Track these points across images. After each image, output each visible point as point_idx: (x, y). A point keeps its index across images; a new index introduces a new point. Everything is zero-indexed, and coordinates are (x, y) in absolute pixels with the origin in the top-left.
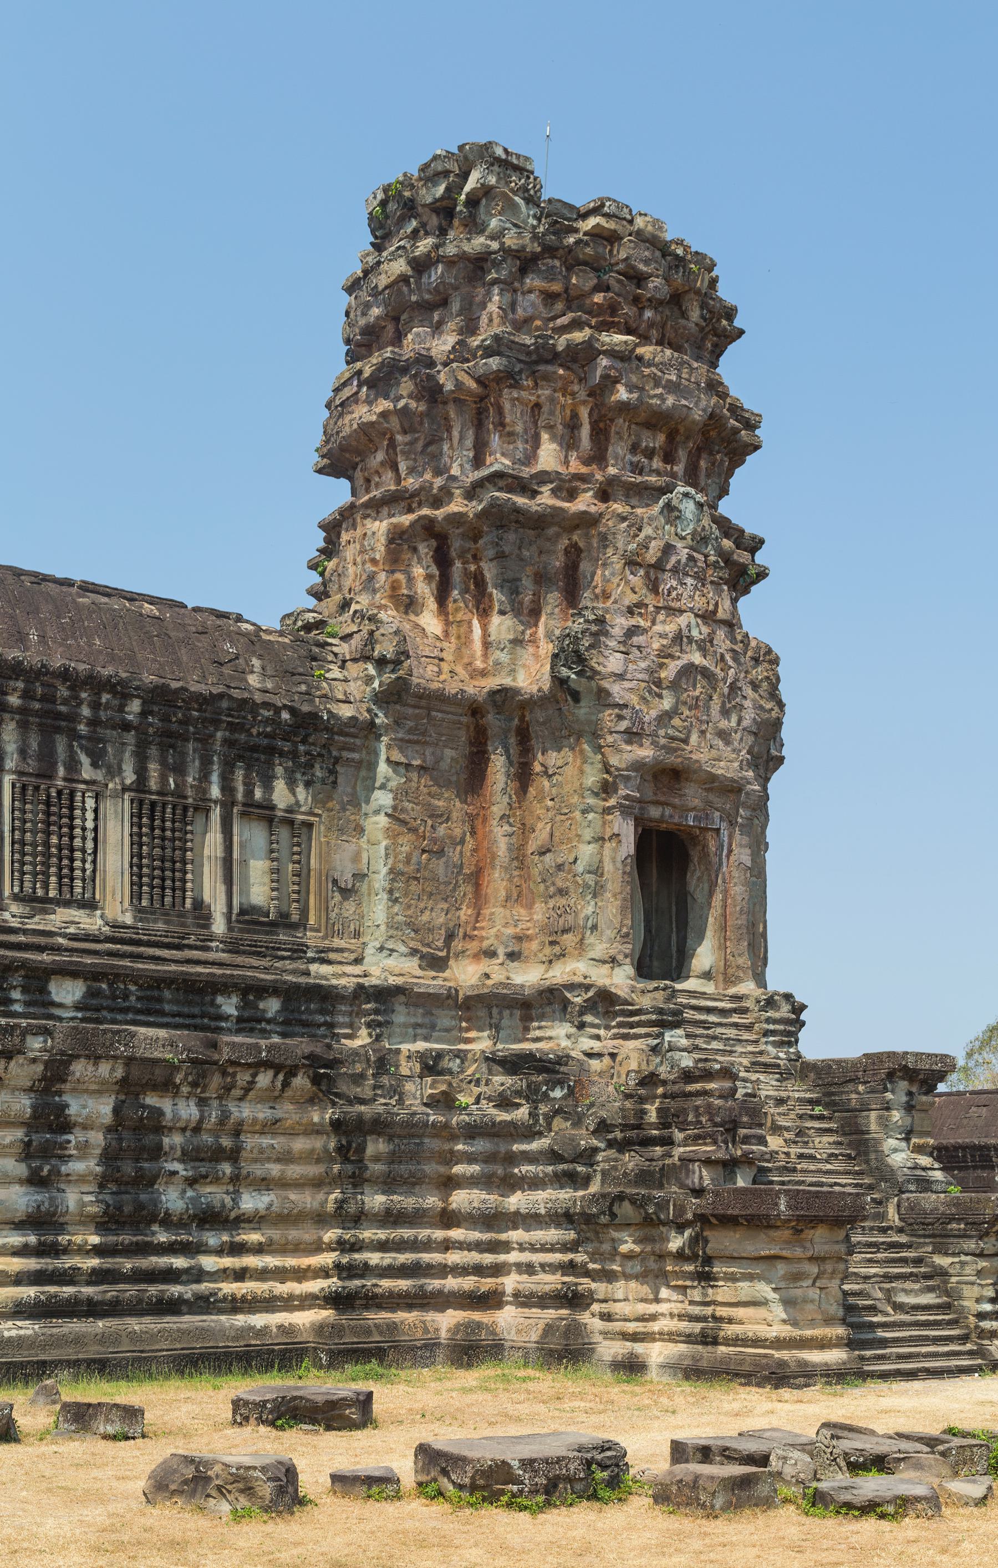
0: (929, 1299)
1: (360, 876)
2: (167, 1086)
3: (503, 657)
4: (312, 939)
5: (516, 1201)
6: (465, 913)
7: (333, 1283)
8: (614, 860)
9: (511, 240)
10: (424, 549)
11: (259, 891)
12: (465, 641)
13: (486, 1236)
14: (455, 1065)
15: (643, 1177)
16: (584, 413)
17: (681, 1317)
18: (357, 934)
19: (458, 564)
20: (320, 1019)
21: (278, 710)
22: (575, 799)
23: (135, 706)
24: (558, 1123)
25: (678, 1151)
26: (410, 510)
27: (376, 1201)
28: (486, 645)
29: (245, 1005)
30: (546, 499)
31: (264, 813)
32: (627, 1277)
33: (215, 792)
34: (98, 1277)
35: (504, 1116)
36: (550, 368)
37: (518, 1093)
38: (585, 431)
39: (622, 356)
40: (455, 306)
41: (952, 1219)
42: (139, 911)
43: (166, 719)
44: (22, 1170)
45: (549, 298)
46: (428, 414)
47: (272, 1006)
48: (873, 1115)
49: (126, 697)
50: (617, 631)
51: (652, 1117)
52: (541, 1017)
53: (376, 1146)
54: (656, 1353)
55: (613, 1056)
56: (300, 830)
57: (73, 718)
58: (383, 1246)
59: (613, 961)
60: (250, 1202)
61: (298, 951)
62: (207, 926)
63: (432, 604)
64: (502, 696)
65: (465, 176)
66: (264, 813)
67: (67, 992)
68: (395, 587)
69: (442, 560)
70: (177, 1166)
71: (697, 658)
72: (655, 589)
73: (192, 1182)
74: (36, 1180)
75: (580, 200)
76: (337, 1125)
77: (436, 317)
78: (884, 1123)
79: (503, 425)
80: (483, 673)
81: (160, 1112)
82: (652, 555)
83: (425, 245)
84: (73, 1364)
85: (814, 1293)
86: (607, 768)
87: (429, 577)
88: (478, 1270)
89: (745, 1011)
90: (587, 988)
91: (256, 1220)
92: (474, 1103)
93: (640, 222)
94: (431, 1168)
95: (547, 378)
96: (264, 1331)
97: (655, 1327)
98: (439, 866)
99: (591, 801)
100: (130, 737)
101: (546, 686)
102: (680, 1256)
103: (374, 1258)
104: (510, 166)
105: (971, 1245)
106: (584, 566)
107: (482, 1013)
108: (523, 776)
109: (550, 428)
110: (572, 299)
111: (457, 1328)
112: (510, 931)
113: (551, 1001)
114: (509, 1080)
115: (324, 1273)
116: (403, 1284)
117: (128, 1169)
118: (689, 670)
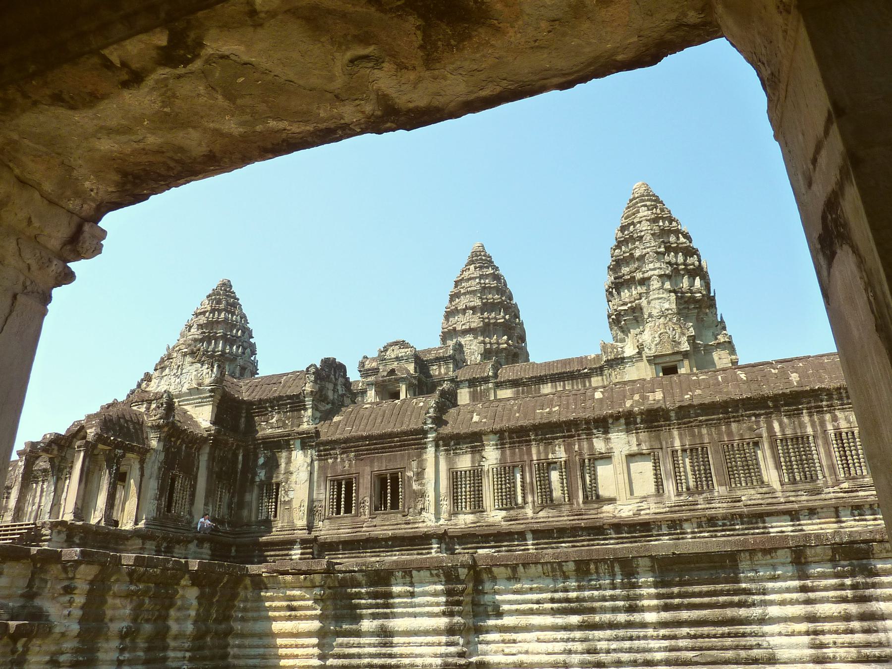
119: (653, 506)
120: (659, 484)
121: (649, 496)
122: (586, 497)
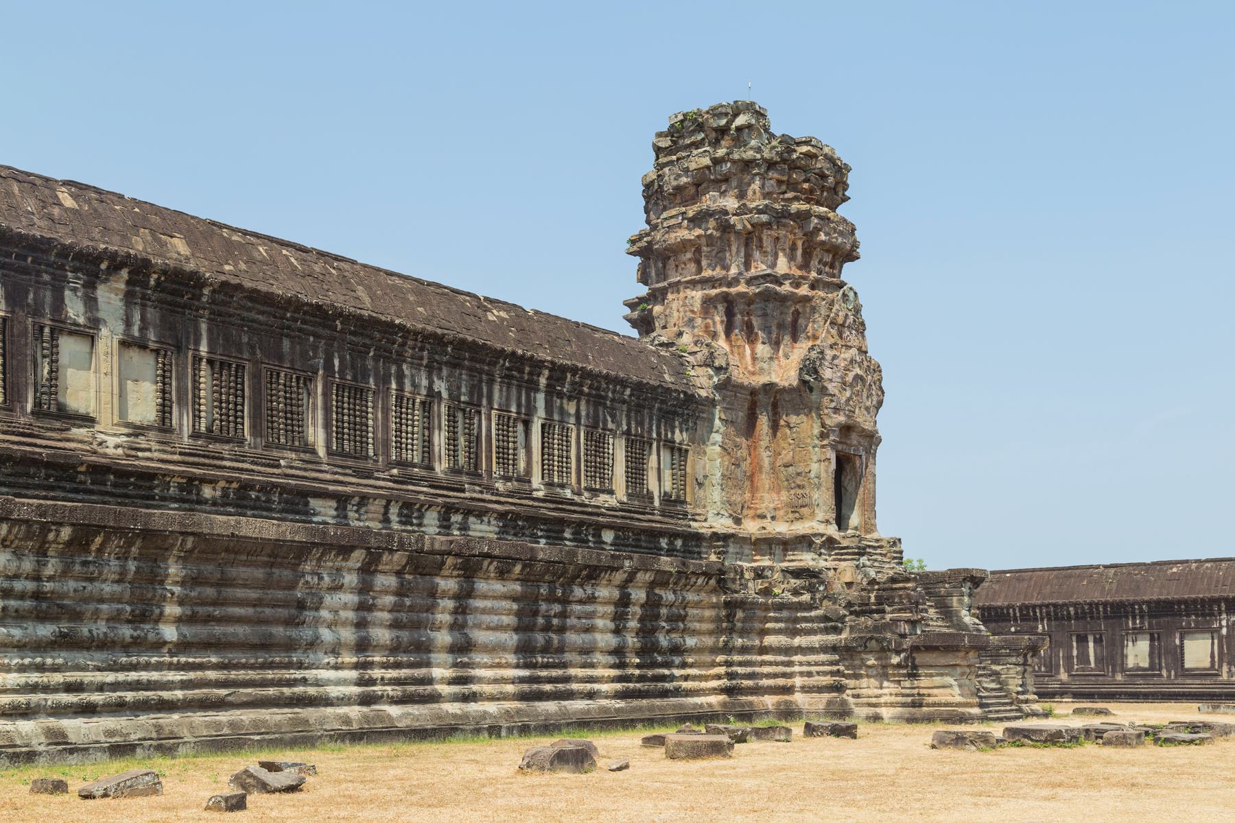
0: (993, 685)
1: (705, 477)
2: (664, 585)
3: (765, 366)
4: (689, 508)
5: (798, 641)
6: (748, 495)
7: (724, 682)
8: (827, 471)
9: (767, 154)
10: (721, 308)
11: (668, 486)
12: (742, 356)
13: (786, 659)
14: (769, 573)
15: (876, 629)
16: (800, 243)
17: (896, 695)
18: (704, 507)
19: (739, 316)
20: (696, 550)
21: (679, 393)
22: (809, 441)
23: (628, 392)
24: (825, 602)
25: (888, 617)
26: (714, 287)
27: (739, 642)
28: (754, 359)
29: (671, 543)
30: (786, 288)
31: (671, 446)
32: (868, 676)
33: (654, 436)
34: (641, 679)
35: (795, 599)
36: (787, 221)
37: (803, 588)
38: (799, 252)
39: (823, 218)
40: (734, 184)
41: (1003, 648)
42: (629, 495)
43: (638, 398)
44: (611, 625)
45: (780, 182)
46: (720, 238)
47: (679, 543)
48: (955, 599)
49: (625, 387)
50: (828, 358)
51: (873, 600)
53: (740, 614)
54: (885, 712)
55: (835, 569)
56: (683, 453)
57: (605, 398)
58: (741, 664)
59: (827, 521)
60: (691, 642)
61: (685, 514)
62: (652, 503)
63: (723, 336)
64: (769, 387)
65: (736, 115)
66: (671, 446)
67: (608, 536)
68: (707, 326)
69: (730, 314)
70: (664, 624)
71: (858, 371)
72: (841, 337)
73: (668, 632)
74: (617, 632)
75: (797, 135)
76: (727, 604)
77: (723, 188)
78: (961, 602)
79: (761, 247)
80: (753, 374)
81: (661, 597)
82: (840, 320)
83: (721, 152)
84: (642, 721)
85: (967, 682)
86: (823, 425)
87: (722, 322)
88: (784, 675)
89: (881, 547)
90: (822, 535)
91: (691, 651)
92: (783, 591)
93: (826, 150)
94: (757, 625)
95: (785, 225)
96: (701, 706)
97: (882, 700)
98: (738, 471)
99: (816, 442)
100: (625, 407)
101: (795, 383)
102: (899, 666)
103: (740, 670)
104: (760, 114)
105: (1014, 660)
106: (801, 321)
107: (764, 547)
108: (775, 427)
109: (783, 250)
110: (793, 186)
111: (779, 704)
112: (772, 505)
113: (805, 542)
114: (798, 582)
115: (719, 677)
116: (750, 683)
117: (649, 625)
118: (857, 377)
119: (155, 446)
120: (164, 409)
121: (149, 428)
122: (38, 404)
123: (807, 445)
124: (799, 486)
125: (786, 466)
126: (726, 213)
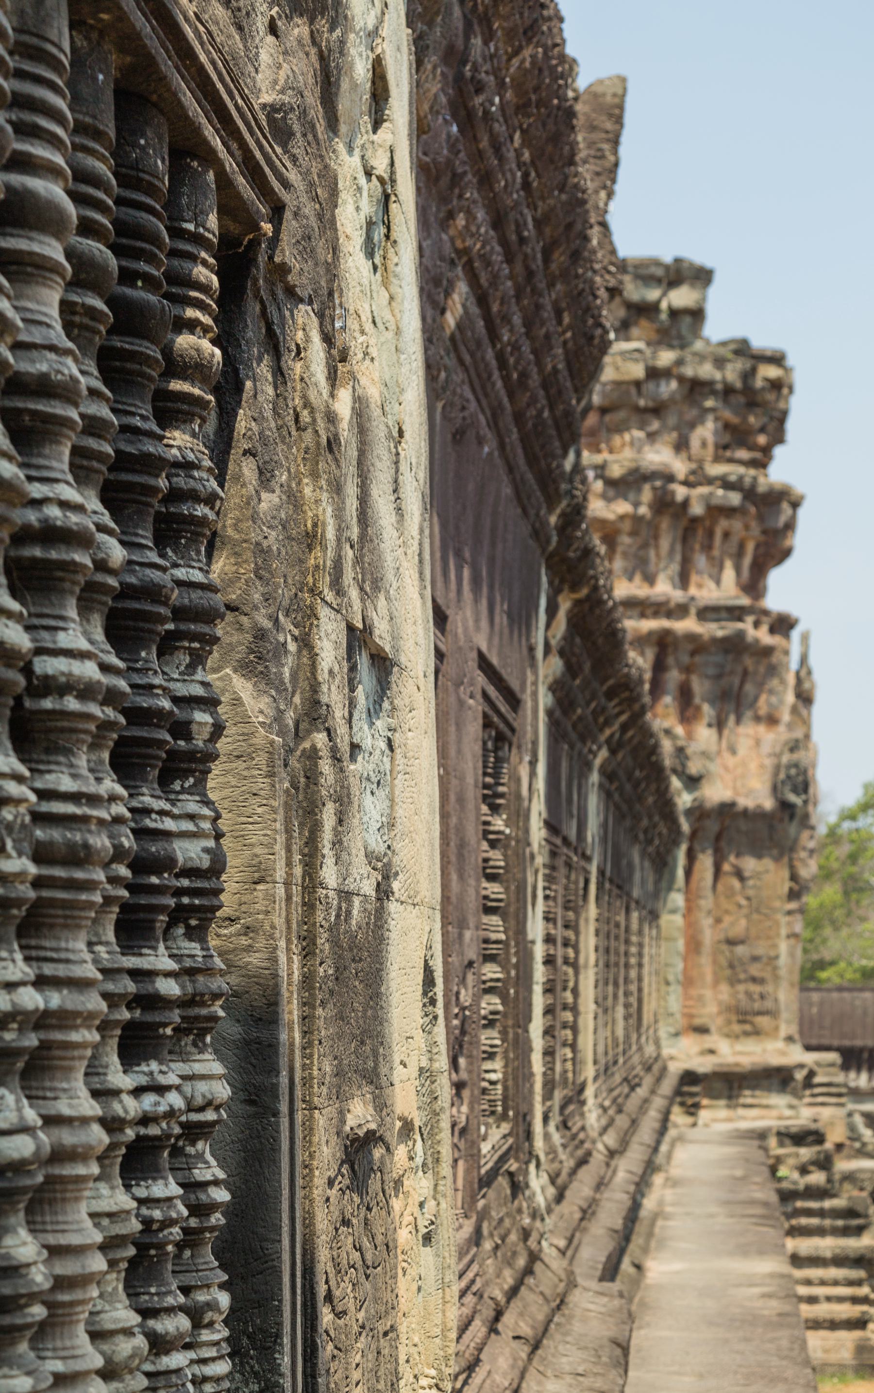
26: (643, 616)
52: (753, 1088)
90: (801, 1066)
113: (778, 1078)
123: (775, 910)
124: (754, 980)
125: (731, 942)
126: (670, 478)
